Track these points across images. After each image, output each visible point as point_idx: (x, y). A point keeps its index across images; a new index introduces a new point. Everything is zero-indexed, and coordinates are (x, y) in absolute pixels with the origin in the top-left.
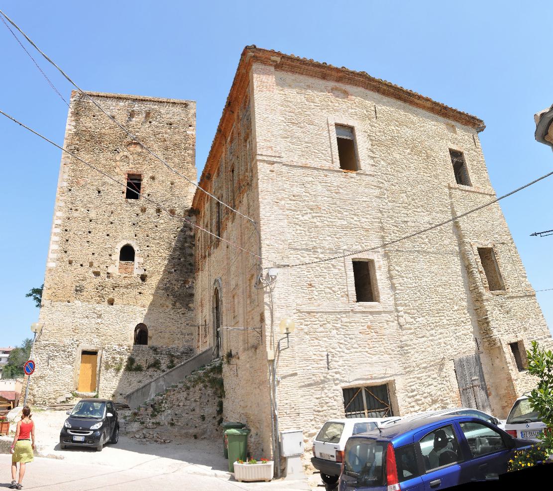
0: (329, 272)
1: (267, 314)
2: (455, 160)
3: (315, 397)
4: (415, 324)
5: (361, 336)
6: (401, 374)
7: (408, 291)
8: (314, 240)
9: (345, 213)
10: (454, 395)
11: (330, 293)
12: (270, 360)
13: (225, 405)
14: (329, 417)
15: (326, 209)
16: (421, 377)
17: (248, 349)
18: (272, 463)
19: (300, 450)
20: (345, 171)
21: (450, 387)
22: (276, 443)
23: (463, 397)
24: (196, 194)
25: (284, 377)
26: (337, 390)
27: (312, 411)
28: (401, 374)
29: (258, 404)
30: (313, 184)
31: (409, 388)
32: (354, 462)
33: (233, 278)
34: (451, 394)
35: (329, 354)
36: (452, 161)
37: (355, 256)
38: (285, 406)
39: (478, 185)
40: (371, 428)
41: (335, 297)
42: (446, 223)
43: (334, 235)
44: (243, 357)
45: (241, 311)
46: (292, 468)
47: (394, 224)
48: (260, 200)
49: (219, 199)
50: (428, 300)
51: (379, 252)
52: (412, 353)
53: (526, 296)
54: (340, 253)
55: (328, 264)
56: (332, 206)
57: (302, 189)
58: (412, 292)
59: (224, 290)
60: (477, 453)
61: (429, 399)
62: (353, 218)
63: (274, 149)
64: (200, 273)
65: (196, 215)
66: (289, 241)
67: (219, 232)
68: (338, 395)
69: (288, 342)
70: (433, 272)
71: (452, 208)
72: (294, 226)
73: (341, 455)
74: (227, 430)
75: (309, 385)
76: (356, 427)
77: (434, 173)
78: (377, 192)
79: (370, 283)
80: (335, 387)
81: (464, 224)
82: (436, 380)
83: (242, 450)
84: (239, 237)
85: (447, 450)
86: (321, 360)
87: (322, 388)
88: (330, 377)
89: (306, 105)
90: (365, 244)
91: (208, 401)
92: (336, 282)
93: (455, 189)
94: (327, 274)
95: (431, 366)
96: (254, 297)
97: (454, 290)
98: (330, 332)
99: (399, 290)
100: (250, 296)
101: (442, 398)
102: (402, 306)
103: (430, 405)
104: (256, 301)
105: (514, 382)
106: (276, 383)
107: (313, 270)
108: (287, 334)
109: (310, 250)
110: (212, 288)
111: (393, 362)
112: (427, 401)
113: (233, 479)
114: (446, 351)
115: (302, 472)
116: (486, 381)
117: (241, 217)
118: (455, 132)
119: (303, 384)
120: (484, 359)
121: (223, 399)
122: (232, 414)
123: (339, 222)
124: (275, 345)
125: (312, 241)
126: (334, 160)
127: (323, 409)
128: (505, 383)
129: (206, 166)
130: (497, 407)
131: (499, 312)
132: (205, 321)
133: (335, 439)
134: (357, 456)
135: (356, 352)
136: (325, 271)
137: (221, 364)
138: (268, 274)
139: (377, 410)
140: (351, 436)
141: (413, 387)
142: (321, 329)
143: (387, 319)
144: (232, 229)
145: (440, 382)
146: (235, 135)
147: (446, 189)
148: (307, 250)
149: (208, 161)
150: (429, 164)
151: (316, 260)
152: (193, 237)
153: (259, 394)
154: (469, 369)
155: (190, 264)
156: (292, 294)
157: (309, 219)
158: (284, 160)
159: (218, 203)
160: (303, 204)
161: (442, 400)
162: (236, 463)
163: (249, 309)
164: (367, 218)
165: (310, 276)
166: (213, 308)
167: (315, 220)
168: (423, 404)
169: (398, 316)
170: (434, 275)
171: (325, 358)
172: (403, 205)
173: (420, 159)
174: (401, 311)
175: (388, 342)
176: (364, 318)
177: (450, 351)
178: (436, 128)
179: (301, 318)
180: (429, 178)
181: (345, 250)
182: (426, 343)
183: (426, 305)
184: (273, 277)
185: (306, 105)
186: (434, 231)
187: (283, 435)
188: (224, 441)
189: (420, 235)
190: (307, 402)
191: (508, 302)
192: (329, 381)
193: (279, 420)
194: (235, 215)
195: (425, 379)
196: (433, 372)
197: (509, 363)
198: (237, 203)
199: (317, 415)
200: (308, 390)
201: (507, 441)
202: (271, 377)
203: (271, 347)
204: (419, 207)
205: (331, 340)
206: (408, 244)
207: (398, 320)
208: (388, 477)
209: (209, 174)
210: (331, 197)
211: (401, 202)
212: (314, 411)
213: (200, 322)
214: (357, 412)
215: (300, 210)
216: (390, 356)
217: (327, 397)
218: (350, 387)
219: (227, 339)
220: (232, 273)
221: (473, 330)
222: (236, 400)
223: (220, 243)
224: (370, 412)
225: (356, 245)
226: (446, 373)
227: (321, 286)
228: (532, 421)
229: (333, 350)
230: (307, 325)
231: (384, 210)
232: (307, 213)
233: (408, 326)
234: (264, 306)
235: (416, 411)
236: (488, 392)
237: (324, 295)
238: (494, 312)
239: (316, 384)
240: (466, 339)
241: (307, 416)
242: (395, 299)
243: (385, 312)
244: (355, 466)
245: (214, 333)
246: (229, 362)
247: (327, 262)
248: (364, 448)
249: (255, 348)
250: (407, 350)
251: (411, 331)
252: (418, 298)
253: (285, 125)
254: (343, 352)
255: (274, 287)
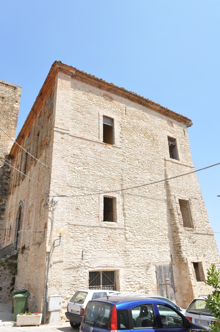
0: (89, 202)
1: (49, 224)
2: (171, 143)
3: (72, 276)
4: (135, 239)
5: (103, 241)
6: (124, 267)
7: (133, 219)
8: (82, 182)
9: (103, 169)
10: (154, 287)
11: (89, 215)
12: (47, 252)
13: (17, 279)
14: (79, 288)
15: (92, 165)
16: (135, 271)
17: (35, 245)
18: (41, 315)
19: (59, 307)
20: (106, 144)
21: (151, 281)
22: (45, 302)
23: (159, 289)
24: (13, 146)
25: (55, 263)
26: (86, 272)
27: (70, 284)
28: (124, 267)
29: (37, 279)
30: (86, 149)
31: (127, 276)
32: (90, 316)
33: (30, 201)
34: (151, 286)
35: (84, 250)
36: (169, 143)
37: (106, 194)
38: (53, 281)
39: (184, 160)
40: (103, 296)
41: (91, 217)
42: (160, 181)
43: (95, 181)
44: (32, 249)
45: (33, 220)
46: (53, 318)
47: (129, 178)
48: (53, 155)
49: (27, 151)
50: (144, 226)
51: (119, 193)
52: (131, 256)
53: (207, 234)
54: (97, 191)
55: (89, 197)
56: (96, 163)
57: (79, 151)
58: (135, 220)
59: (25, 207)
60: (166, 325)
61: (138, 286)
62: (107, 172)
63: (65, 125)
64: (11, 196)
65: (12, 159)
66: (68, 181)
67: (25, 171)
68: (86, 275)
69: (60, 242)
70: (149, 210)
71: (165, 173)
72: (72, 173)
73: (84, 311)
74: (16, 295)
75: (69, 269)
76: (94, 295)
77: (157, 150)
78: (121, 158)
79: (112, 211)
80: (85, 271)
81: (171, 183)
82: (143, 275)
83: (23, 307)
84: (38, 175)
85: (147, 319)
86: (78, 254)
87: (77, 270)
88: (83, 265)
89: (87, 102)
90: (112, 188)
91: (5, 278)
92: (93, 208)
93: (169, 161)
94: (88, 203)
95: (141, 266)
96: (42, 213)
97: (161, 223)
98: (86, 238)
99: (128, 217)
100: (40, 212)
101: (146, 287)
102: (129, 227)
103: (138, 289)
104: (43, 215)
105: (193, 287)
106: (49, 266)
107: (80, 200)
108: (60, 237)
109: (79, 188)
110: (18, 206)
111: (120, 258)
112: (137, 287)
113: (15, 325)
114: (152, 259)
115: (59, 321)
116: (175, 283)
117: (40, 164)
118: (172, 126)
119: (66, 268)
120: (175, 268)
121: (16, 276)
122: (20, 285)
123: (99, 173)
124: (52, 243)
125: (82, 183)
126: (100, 136)
127: (76, 283)
128: (187, 287)
129: (22, 130)
130: (180, 301)
131: (188, 241)
132: (11, 227)
133: (81, 301)
134: (92, 312)
135: (100, 251)
136: (87, 201)
137: (18, 254)
138: (52, 200)
139: (108, 286)
140: (91, 300)
141: (129, 276)
142: (81, 236)
143: (120, 232)
144: (33, 171)
145: (146, 277)
146: (42, 113)
147: (163, 161)
148: (78, 188)
149: (23, 127)
150: (154, 144)
151: (83, 194)
152: (9, 173)
153: (38, 272)
154: (165, 273)
155: (5, 190)
156: (66, 213)
157: (81, 169)
158: (71, 133)
159: (27, 154)
160: (79, 160)
161: (146, 288)
162: (18, 315)
163: (38, 220)
164: (115, 173)
165: (78, 204)
166: (17, 219)
167: (85, 171)
168: (134, 287)
169: (125, 233)
170: (149, 211)
171: (81, 253)
172: (136, 167)
173: (149, 141)
174: (128, 230)
175: (119, 246)
176: (107, 231)
177: (154, 260)
178: (161, 122)
179: (69, 228)
180: (153, 153)
181: (100, 190)
182: (140, 252)
183: (143, 229)
184: (56, 202)
185: (87, 102)
186: (152, 185)
187: (50, 298)
188: (13, 302)
189: (144, 187)
190: (67, 279)
191: (194, 236)
192: (82, 267)
193: (49, 288)
194: (37, 162)
195: (137, 273)
196: (143, 270)
197: (191, 275)
198: (39, 155)
199: (72, 287)
200: (69, 271)
201: (186, 323)
202: (47, 263)
203: (49, 244)
204: (145, 170)
205: (86, 243)
206: (136, 191)
207: (125, 235)
208: (112, 325)
209: (23, 135)
210: (96, 158)
211: (134, 165)
212: (71, 284)
213: (7, 227)
214: (96, 286)
215: (76, 164)
216: (118, 254)
217: (79, 276)
218: (94, 271)
219: (23, 238)
220: (30, 197)
221: (170, 249)
222: (24, 276)
223: (25, 178)
224: (104, 286)
225: (107, 188)
226: (150, 272)
227: (84, 210)
228: (203, 315)
229: (86, 249)
230: (73, 233)
231: (124, 169)
232: (80, 166)
233: (130, 240)
234: (48, 219)
235: (129, 291)
236: (175, 289)
237: (85, 216)
238: (185, 241)
239: (74, 268)
240: (165, 254)
241: (66, 287)
242: (125, 222)
243: (119, 228)
244: (90, 318)
245: (15, 234)
246: (22, 253)
247: (89, 196)
248: (97, 308)
249: (39, 244)
250: (128, 254)
251: (132, 243)
252: (138, 224)
253: (73, 112)
254: (92, 250)
255: (55, 208)
